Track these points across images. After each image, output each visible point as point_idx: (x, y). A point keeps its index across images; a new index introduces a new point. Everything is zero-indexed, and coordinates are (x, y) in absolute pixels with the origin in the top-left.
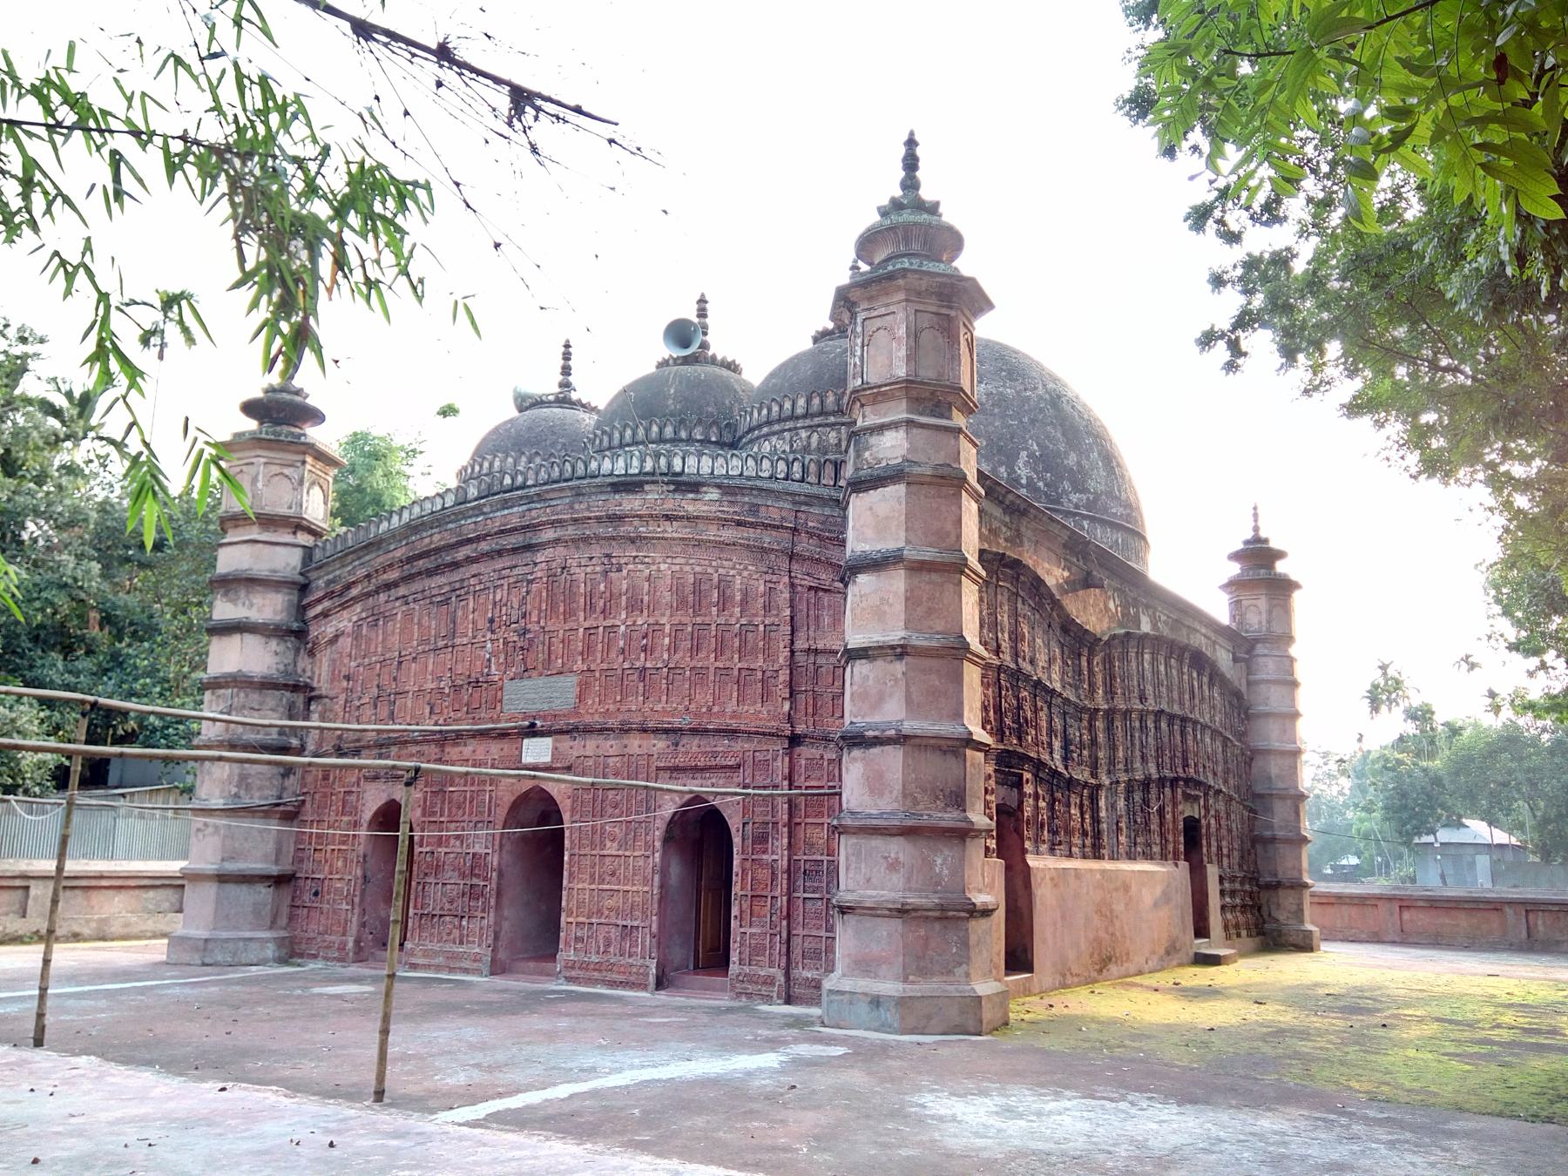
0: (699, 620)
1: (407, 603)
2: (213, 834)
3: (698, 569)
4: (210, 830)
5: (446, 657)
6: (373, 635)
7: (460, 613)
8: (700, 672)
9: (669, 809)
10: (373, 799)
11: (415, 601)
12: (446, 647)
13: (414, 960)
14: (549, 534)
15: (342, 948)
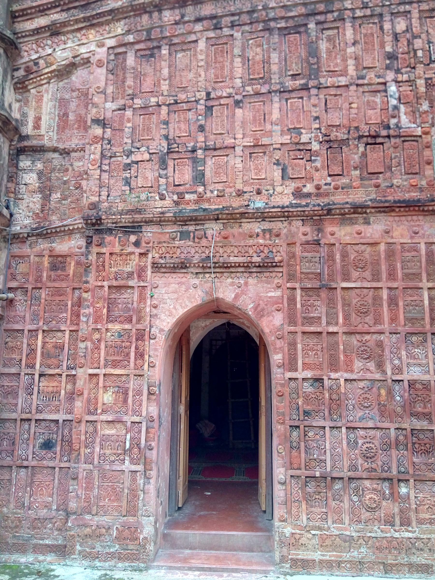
1: (217, 27)
5: (312, 104)
6: (149, 70)
7: (323, 46)
10: (172, 302)
11: (233, 26)
12: (305, 88)
13: (302, 555)
15: (129, 534)
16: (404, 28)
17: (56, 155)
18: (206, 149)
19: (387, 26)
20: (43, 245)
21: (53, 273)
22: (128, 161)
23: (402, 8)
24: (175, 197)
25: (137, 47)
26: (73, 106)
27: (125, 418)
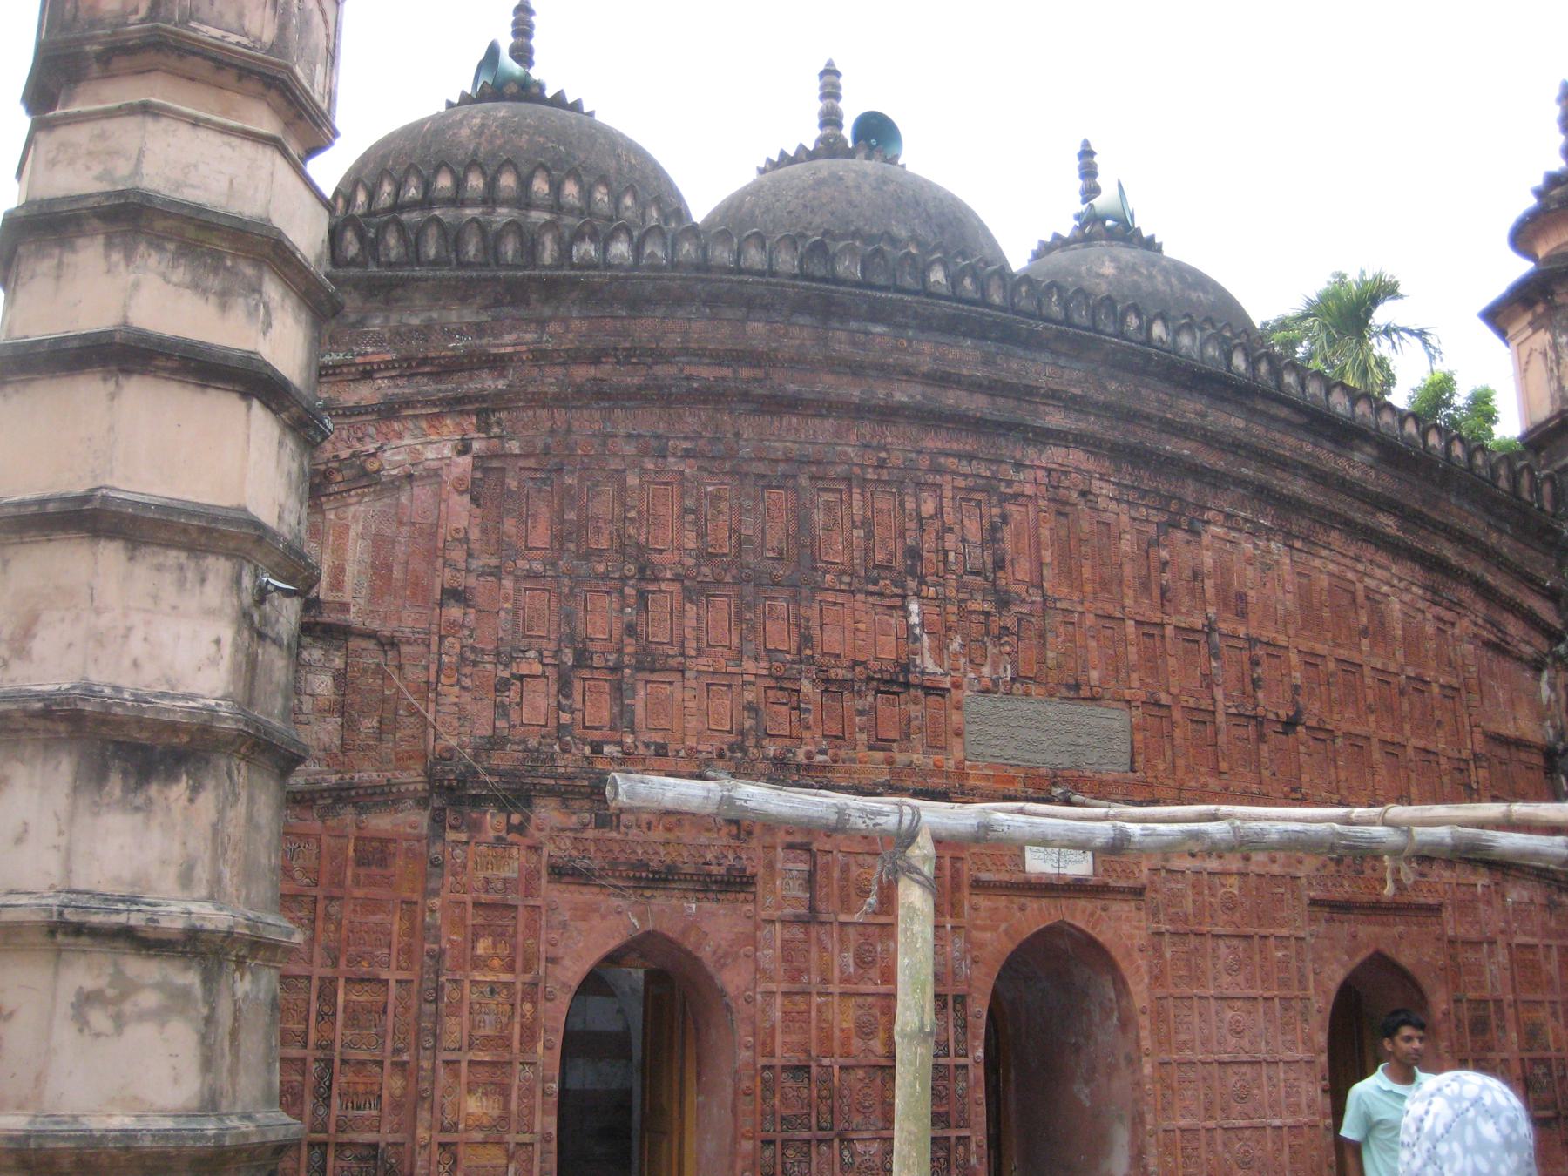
0: (1343, 653)
2: (160, 1016)
3: (1332, 567)
4: (149, 999)
7: (819, 517)
8: (1359, 744)
9: (1336, 974)
14: (1055, 419)
16: (932, 511)
17: (371, 644)
18: (639, 667)
19: (910, 504)
20: (348, 815)
21: (362, 871)
22: (506, 674)
23: (930, 478)
24: (587, 750)
25: (522, 463)
26: (401, 550)
27: (508, 1137)
